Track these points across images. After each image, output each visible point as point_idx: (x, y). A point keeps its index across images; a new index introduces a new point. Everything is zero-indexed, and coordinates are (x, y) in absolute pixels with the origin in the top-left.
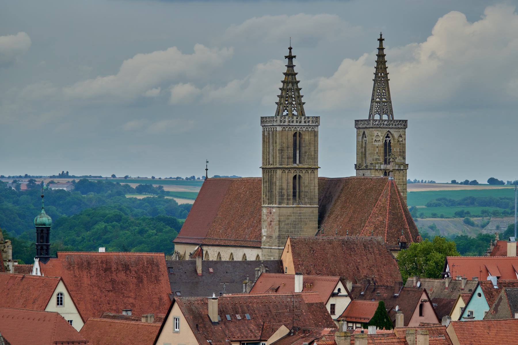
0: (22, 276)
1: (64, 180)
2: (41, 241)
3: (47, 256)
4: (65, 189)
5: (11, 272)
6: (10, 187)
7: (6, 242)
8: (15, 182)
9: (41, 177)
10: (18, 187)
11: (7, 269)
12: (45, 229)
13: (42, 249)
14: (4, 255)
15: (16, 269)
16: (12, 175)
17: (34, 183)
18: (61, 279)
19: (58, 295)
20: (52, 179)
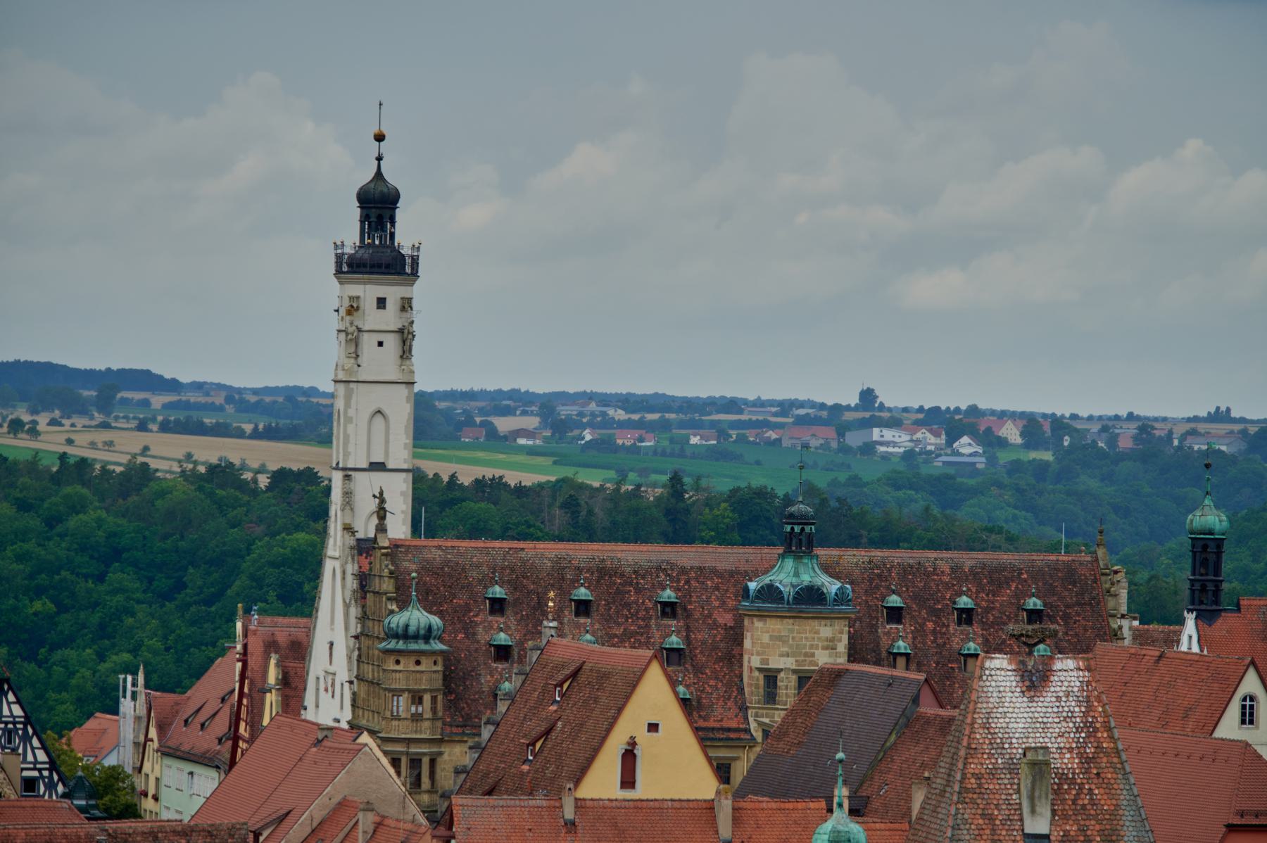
0: (1157, 654)
1: (1224, 428)
2: (1203, 571)
3: (1214, 607)
4: (1224, 448)
5: (1127, 642)
6: (1094, 442)
7: (1116, 572)
8: (1105, 429)
9: (1165, 419)
10: (1113, 441)
11: (1116, 635)
12: (1212, 544)
13: (1204, 589)
14: (1111, 603)
15: (1138, 636)
16: (1096, 413)
17: (1149, 434)
18: (1253, 663)
19: (1244, 699)
20: (1193, 425)
